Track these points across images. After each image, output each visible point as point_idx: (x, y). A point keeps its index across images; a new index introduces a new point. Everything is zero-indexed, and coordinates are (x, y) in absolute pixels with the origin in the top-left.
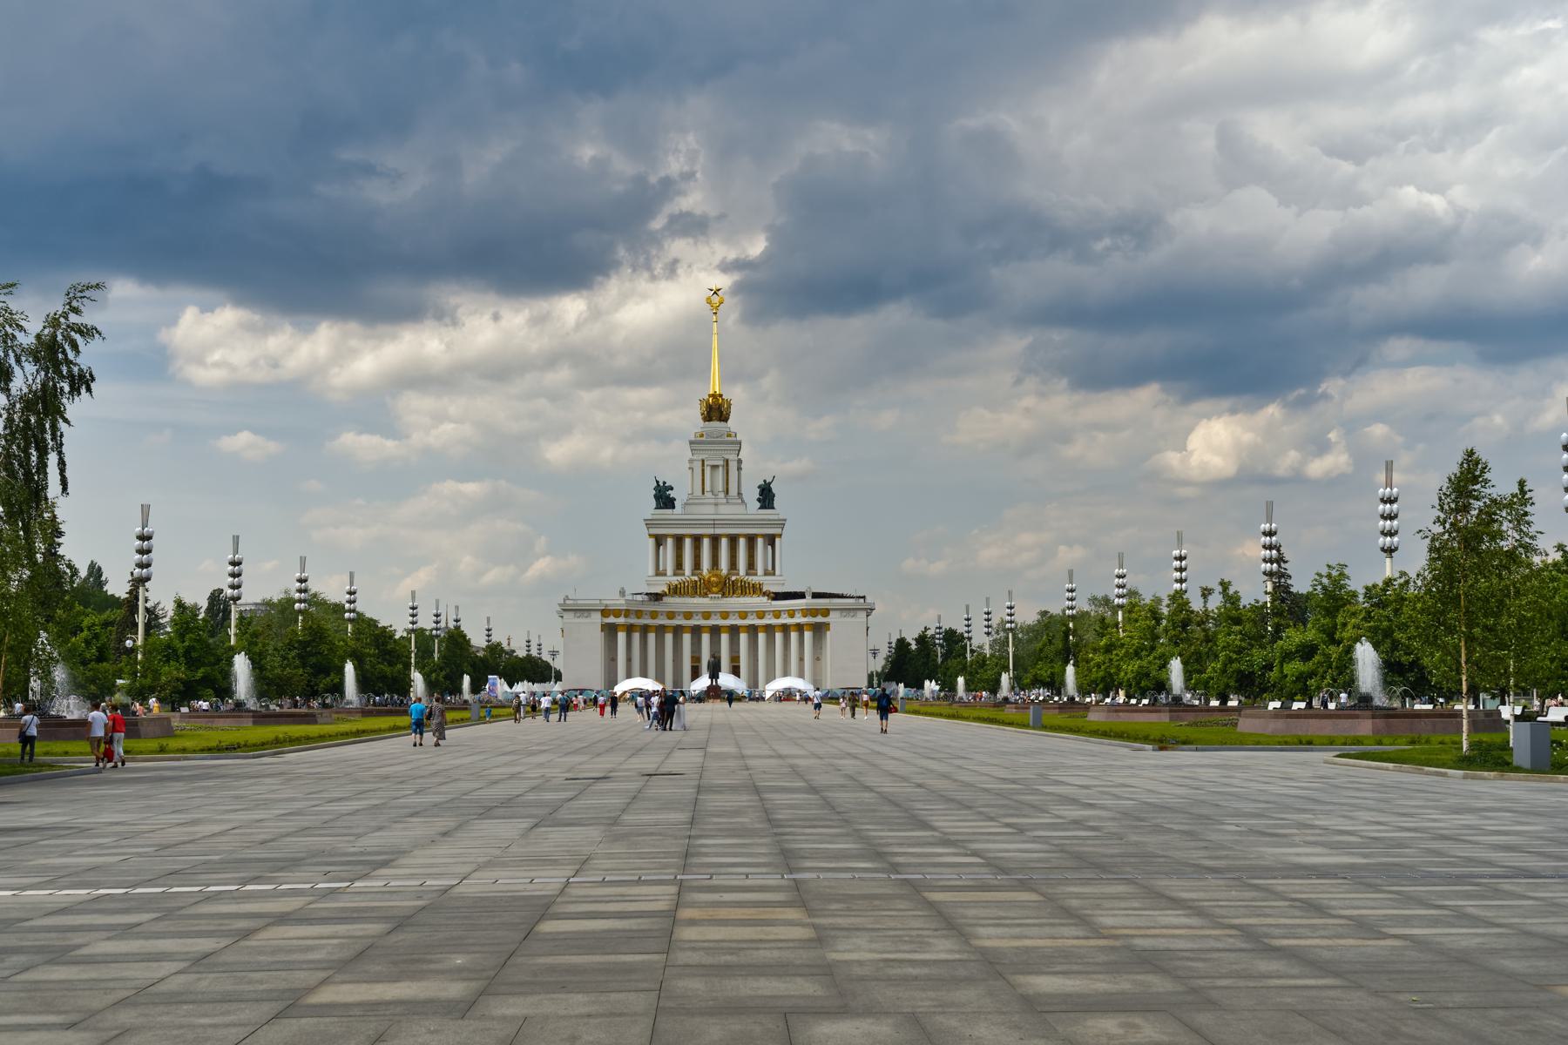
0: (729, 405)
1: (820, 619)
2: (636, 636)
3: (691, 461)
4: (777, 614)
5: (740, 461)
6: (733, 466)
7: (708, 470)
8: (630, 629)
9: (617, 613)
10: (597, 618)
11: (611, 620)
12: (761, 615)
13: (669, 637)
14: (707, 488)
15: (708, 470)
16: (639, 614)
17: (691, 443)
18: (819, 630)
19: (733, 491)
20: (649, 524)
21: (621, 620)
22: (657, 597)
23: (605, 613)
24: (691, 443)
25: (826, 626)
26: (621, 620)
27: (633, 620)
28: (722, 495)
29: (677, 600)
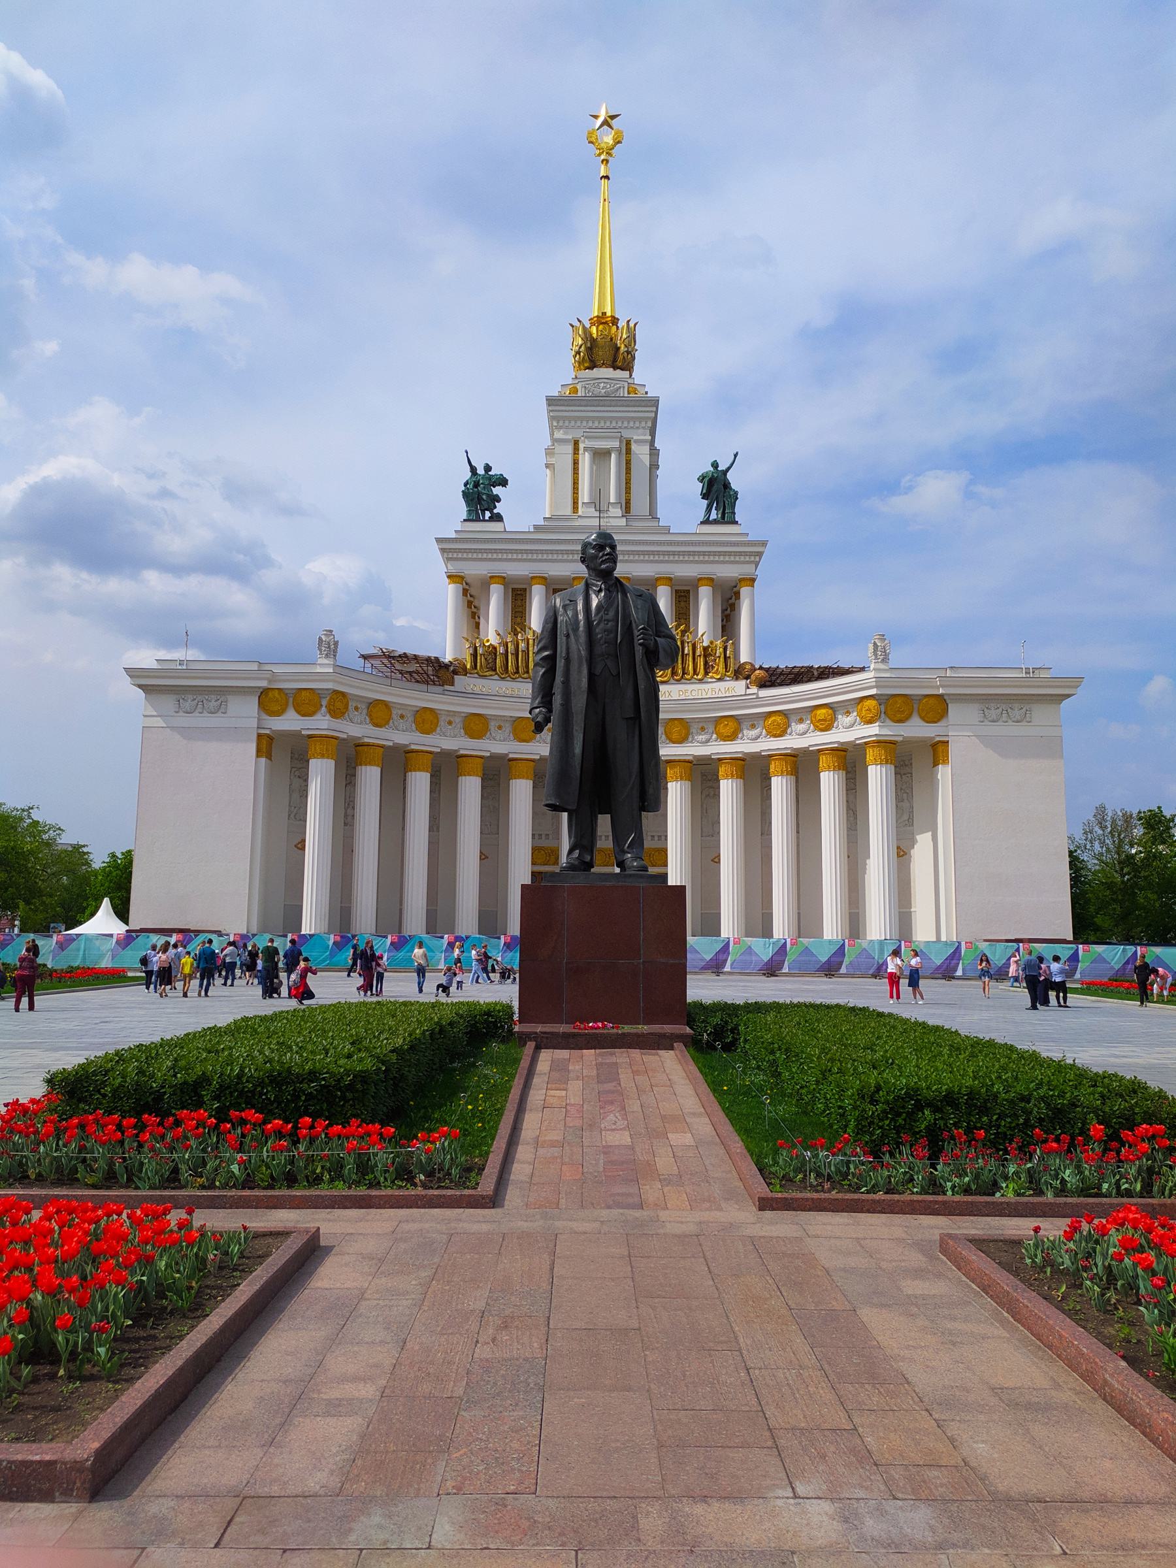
0: (632, 338)
1: (916, 729)
2: (370, 777)
3: (549, 452)
4: (780, 723)
5: (654, 453)
6: (641, 452)
7: (585, 460)
8: (350, 757)
9: (306, 701)
10: (246, 712)
11: (290, 722)
12: (731, 727)
13: (470, 788)
14: (585, 496)
15: (585, 460)
16: (379, 712)
17: (551, 401)
18: (913, 764)
19: (640, 504)
20: (449, 548)
21: (321, 723)
22: (437, 673)
23: (271, 699)
24: (551, 401)
25: (937, 751)
26: (321, 723)
27: (356, 729)
28: (617, 511)
29: (493, 685)
